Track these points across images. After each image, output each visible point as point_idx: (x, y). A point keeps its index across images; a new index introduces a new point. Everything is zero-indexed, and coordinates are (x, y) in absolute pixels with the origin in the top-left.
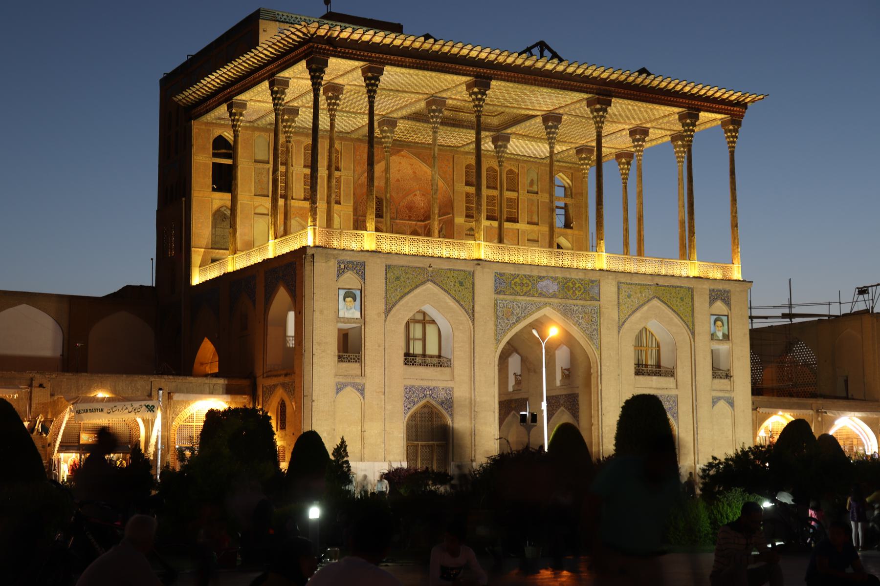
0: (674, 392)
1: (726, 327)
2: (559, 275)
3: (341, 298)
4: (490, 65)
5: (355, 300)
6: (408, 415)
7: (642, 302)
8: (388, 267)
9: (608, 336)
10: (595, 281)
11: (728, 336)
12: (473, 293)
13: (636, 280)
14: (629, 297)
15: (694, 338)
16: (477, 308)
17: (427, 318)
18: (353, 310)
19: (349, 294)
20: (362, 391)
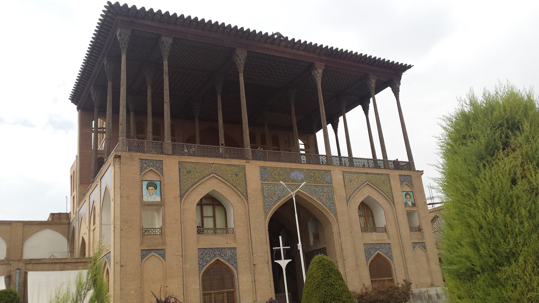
3: (144, 187)
5: (156, 188)
12: (246, 181)
14: (351, 181)
16: (249, 191)
18: (155, 195)
19: (152, 184)
20: (164, 257)
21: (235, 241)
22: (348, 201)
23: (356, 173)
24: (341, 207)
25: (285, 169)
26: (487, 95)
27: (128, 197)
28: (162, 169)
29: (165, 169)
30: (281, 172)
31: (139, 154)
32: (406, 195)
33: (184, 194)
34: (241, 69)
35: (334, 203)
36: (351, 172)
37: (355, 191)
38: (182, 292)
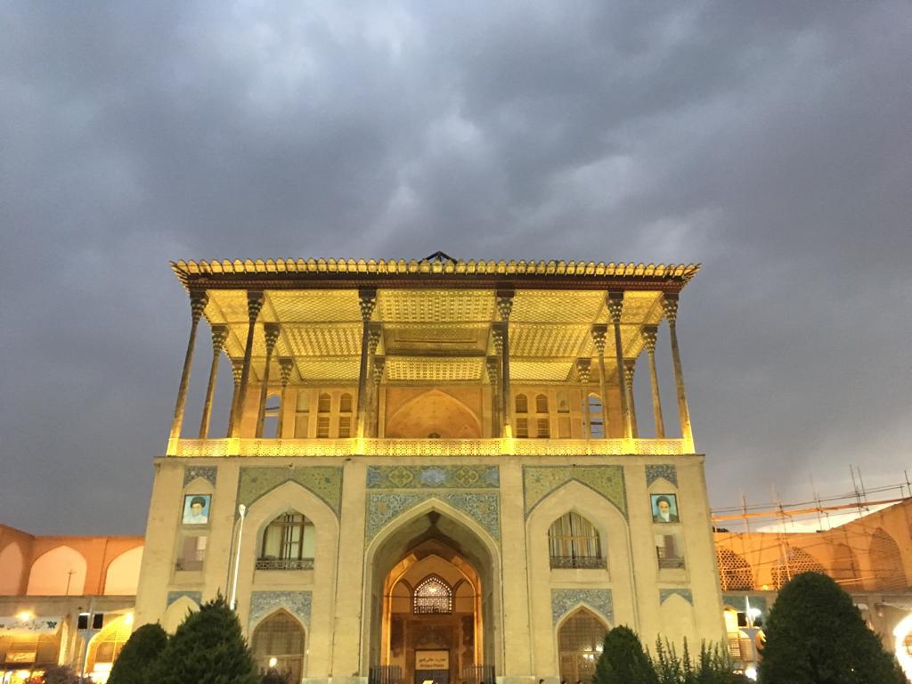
0: (605, 586)
1: (674, 508)
2: (448, 463)
4: (372, 276)
5: (203, 505)
6: (557, 626)
7: (554, 486)
8: (243, 470)
9: (511, 524)
10: (494, 467)
11: (678, 517)
12: (341, 489)
13: (544, 462)
14: (538, 481)
15: (628, 522)
16: (344, 504)
17: (306, 520)
21: (313, 582)
22: (526, 516)
28: (215, 478)
30: (405, 473)
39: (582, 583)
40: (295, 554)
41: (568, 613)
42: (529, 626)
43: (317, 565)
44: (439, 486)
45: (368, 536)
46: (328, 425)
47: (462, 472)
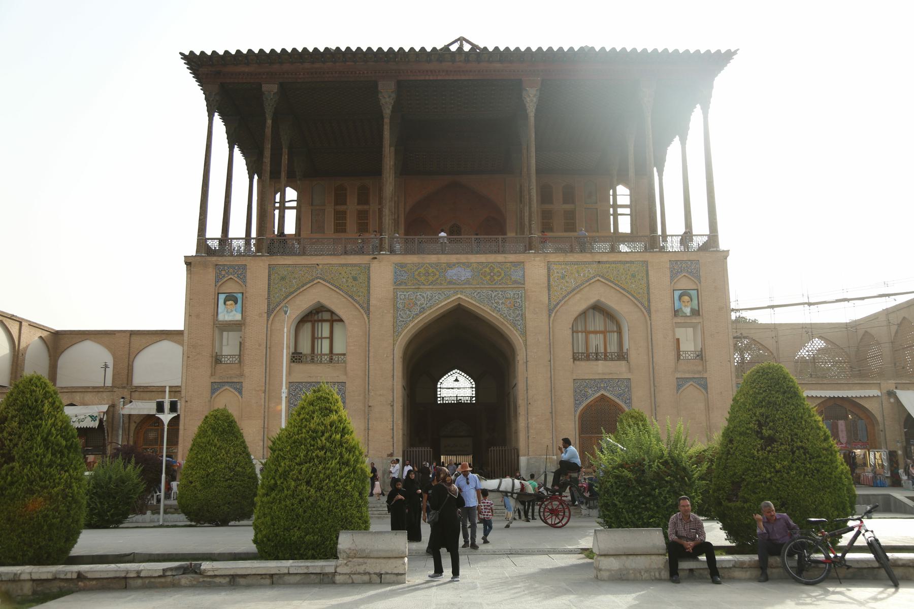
1: (695, 302)
5: (236, 302)
12: (369, 286)
14: (563, 278)
16: (373, 302)
19: (231, 298)
20: (240, 393)
21: (346, 374)
23: (576, 263)
24: (536, 320)
25: (438, 264)
26: (352, 207)
27: (198, 316)
28: (245, 277)
29: (249, 275)
30: (431, 270)
31: (214, 259)
32: (680, 297)
33: (274, 309)
34: (387, 112)
35: (523, 316)
36: (566, 263)
37: (568, 294)
38: (261, 437)
39: (604, 374)
40: (326, 350)
41: (589, 401)
42: (551, 413)
43: (349, 358)
44: (465, 284)
45: (396, 333)
46: (345, 219)
47: (487, 270)
